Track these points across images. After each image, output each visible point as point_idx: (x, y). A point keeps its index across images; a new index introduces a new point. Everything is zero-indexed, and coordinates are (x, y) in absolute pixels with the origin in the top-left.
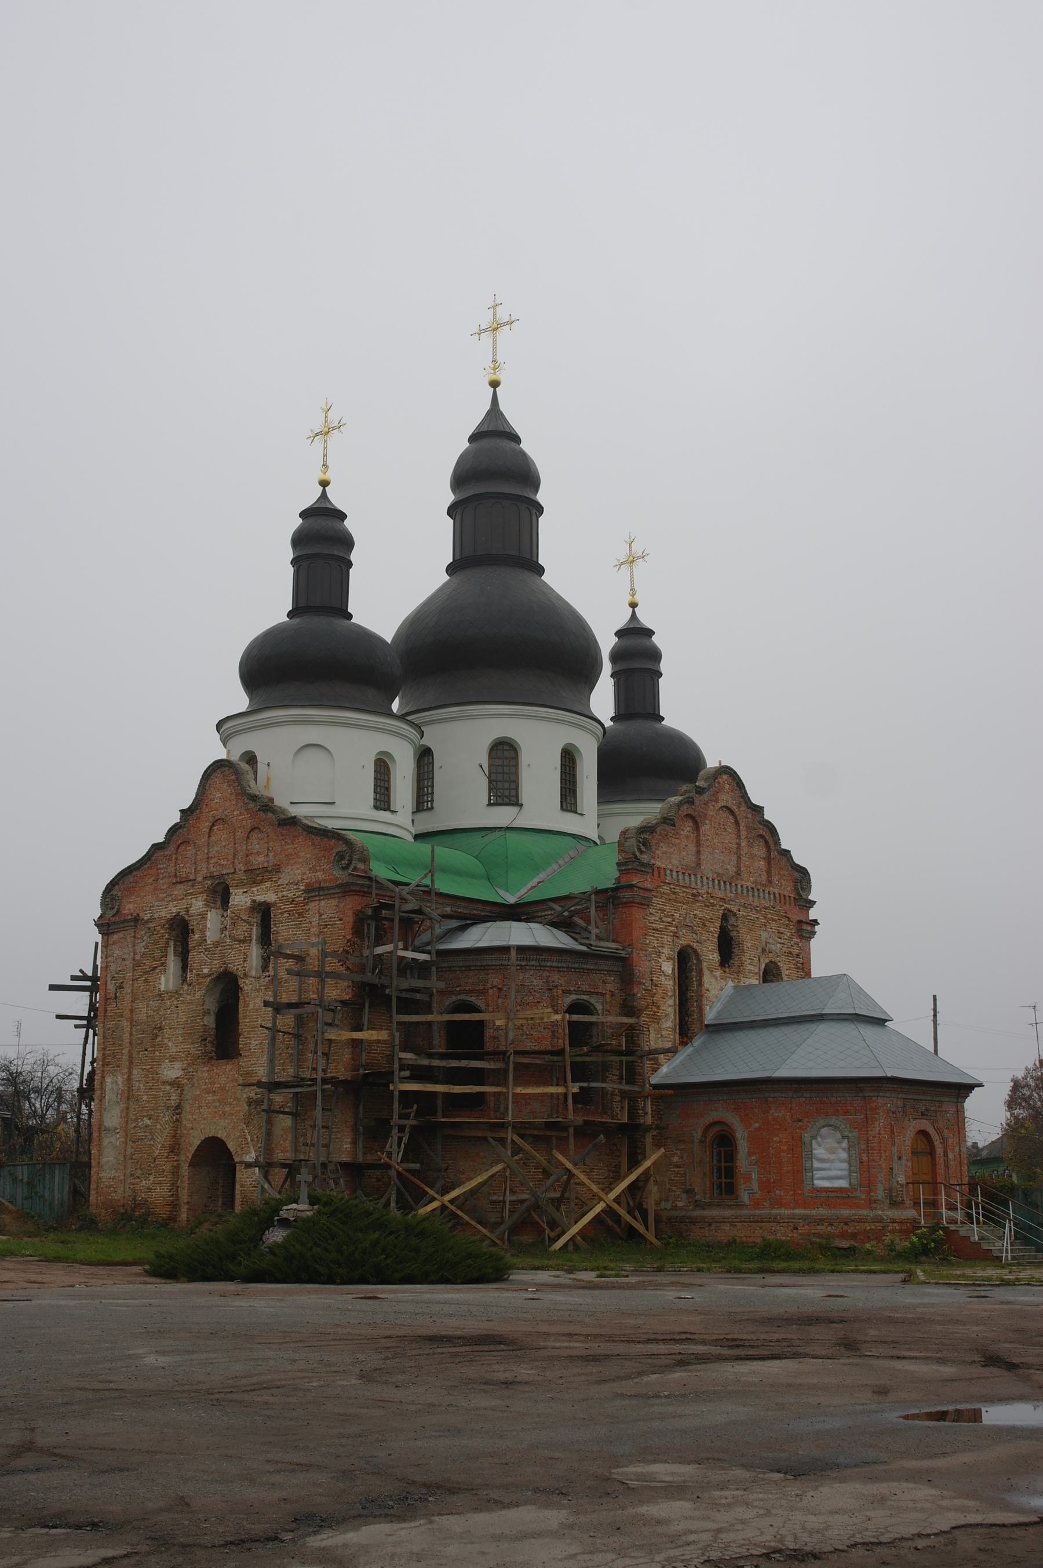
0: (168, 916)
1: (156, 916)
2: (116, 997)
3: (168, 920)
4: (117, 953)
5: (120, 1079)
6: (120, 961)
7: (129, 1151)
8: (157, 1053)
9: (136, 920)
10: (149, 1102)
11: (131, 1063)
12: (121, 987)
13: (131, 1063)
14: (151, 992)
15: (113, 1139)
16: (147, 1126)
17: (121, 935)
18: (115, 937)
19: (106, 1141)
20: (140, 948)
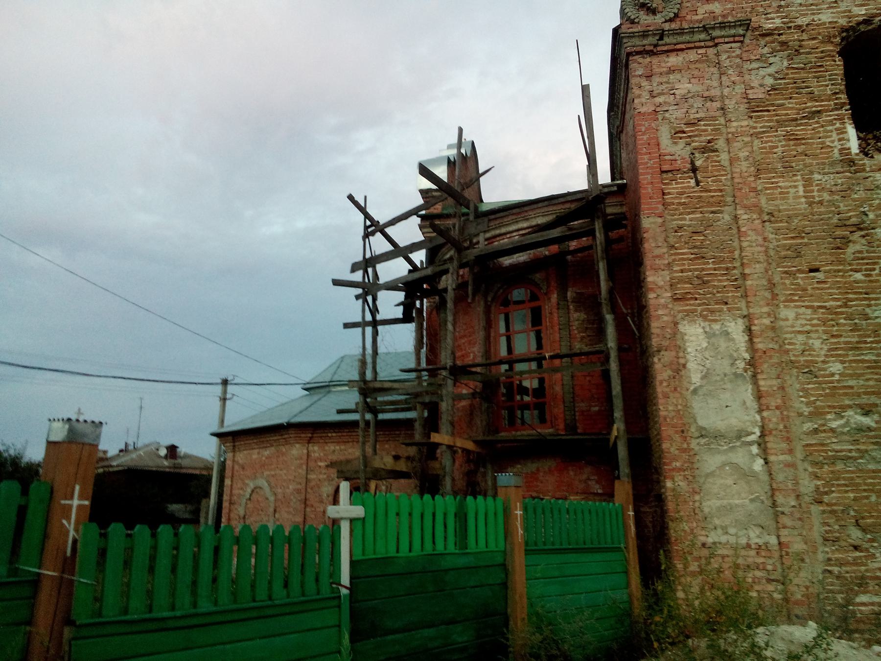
0: (843, 22)
1: (803, 21)
2: (694, 170)
3: (844, 30)
4: (684, 87)
5: (736, 328)
6: (698, 103)
7: (807, 486)
8: (859, 276)
9: (746, 24)
10: (858, 376)
11: (775, 296)
12: (708, 149)
13: (775, 296)
14: (815, 156)
15: (739, 457)
16: (860, 429)
17: (692, 55)
18: (673, 60)
19: (711, 462)
20: (761, 79)
